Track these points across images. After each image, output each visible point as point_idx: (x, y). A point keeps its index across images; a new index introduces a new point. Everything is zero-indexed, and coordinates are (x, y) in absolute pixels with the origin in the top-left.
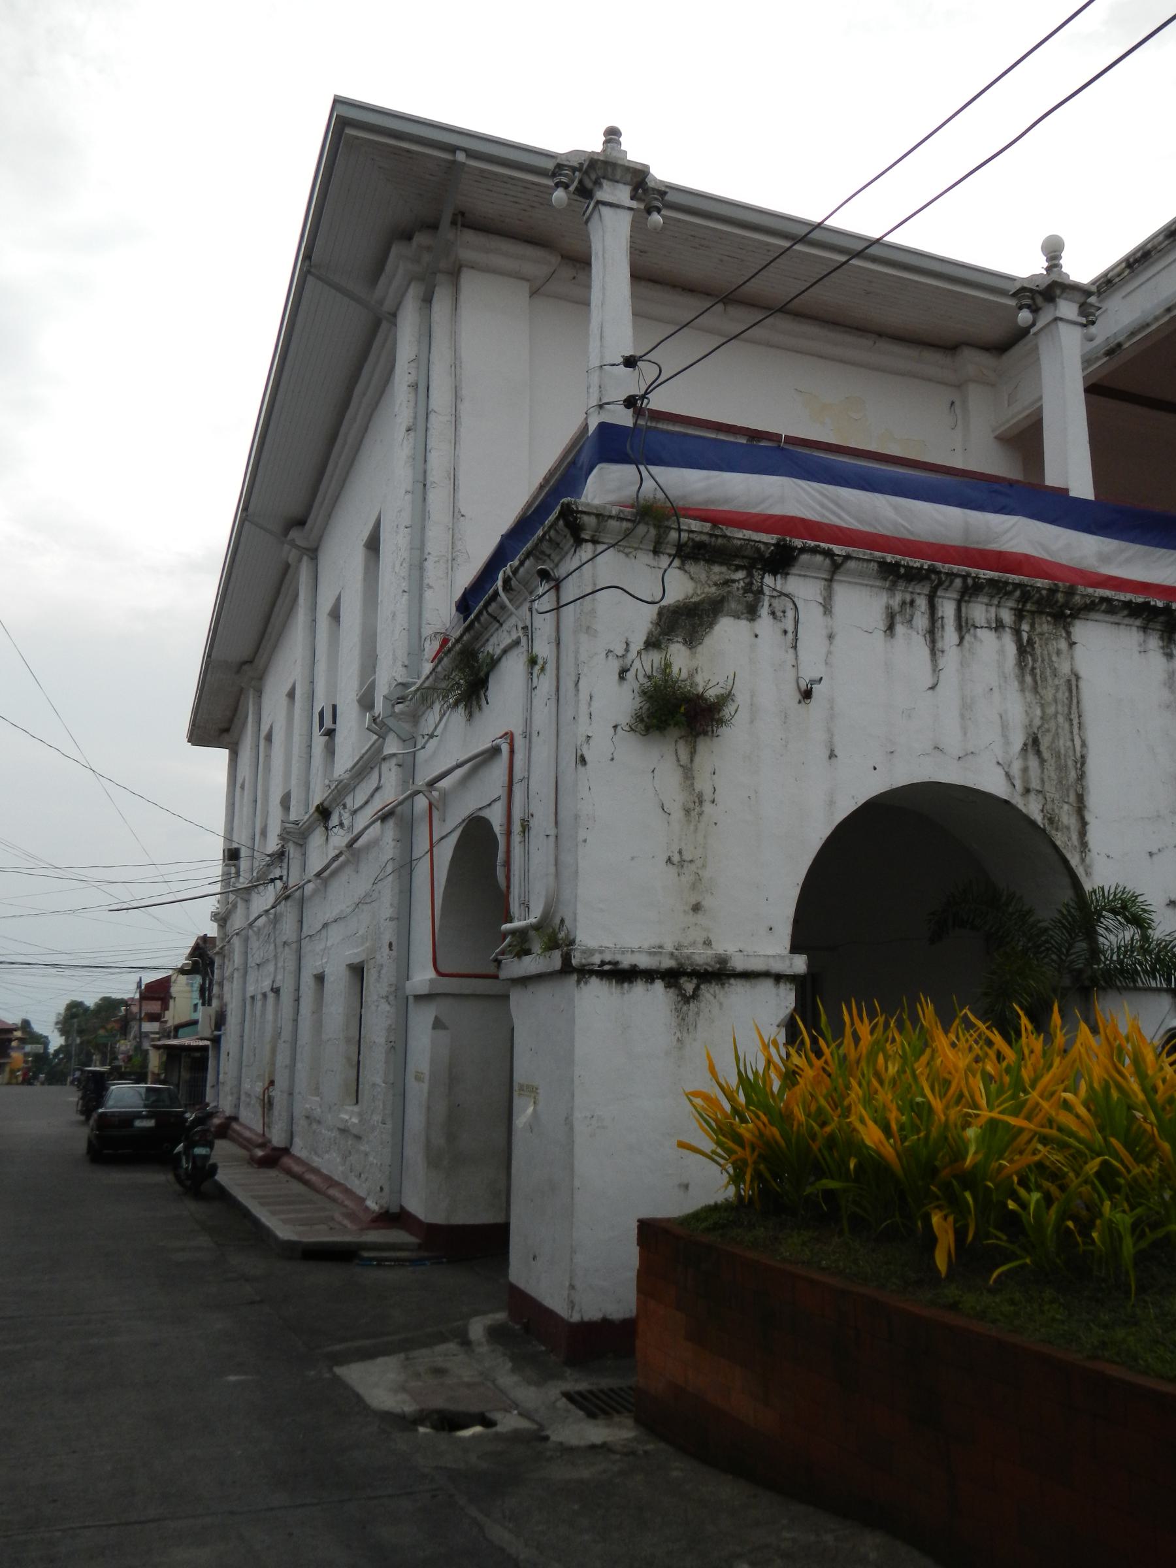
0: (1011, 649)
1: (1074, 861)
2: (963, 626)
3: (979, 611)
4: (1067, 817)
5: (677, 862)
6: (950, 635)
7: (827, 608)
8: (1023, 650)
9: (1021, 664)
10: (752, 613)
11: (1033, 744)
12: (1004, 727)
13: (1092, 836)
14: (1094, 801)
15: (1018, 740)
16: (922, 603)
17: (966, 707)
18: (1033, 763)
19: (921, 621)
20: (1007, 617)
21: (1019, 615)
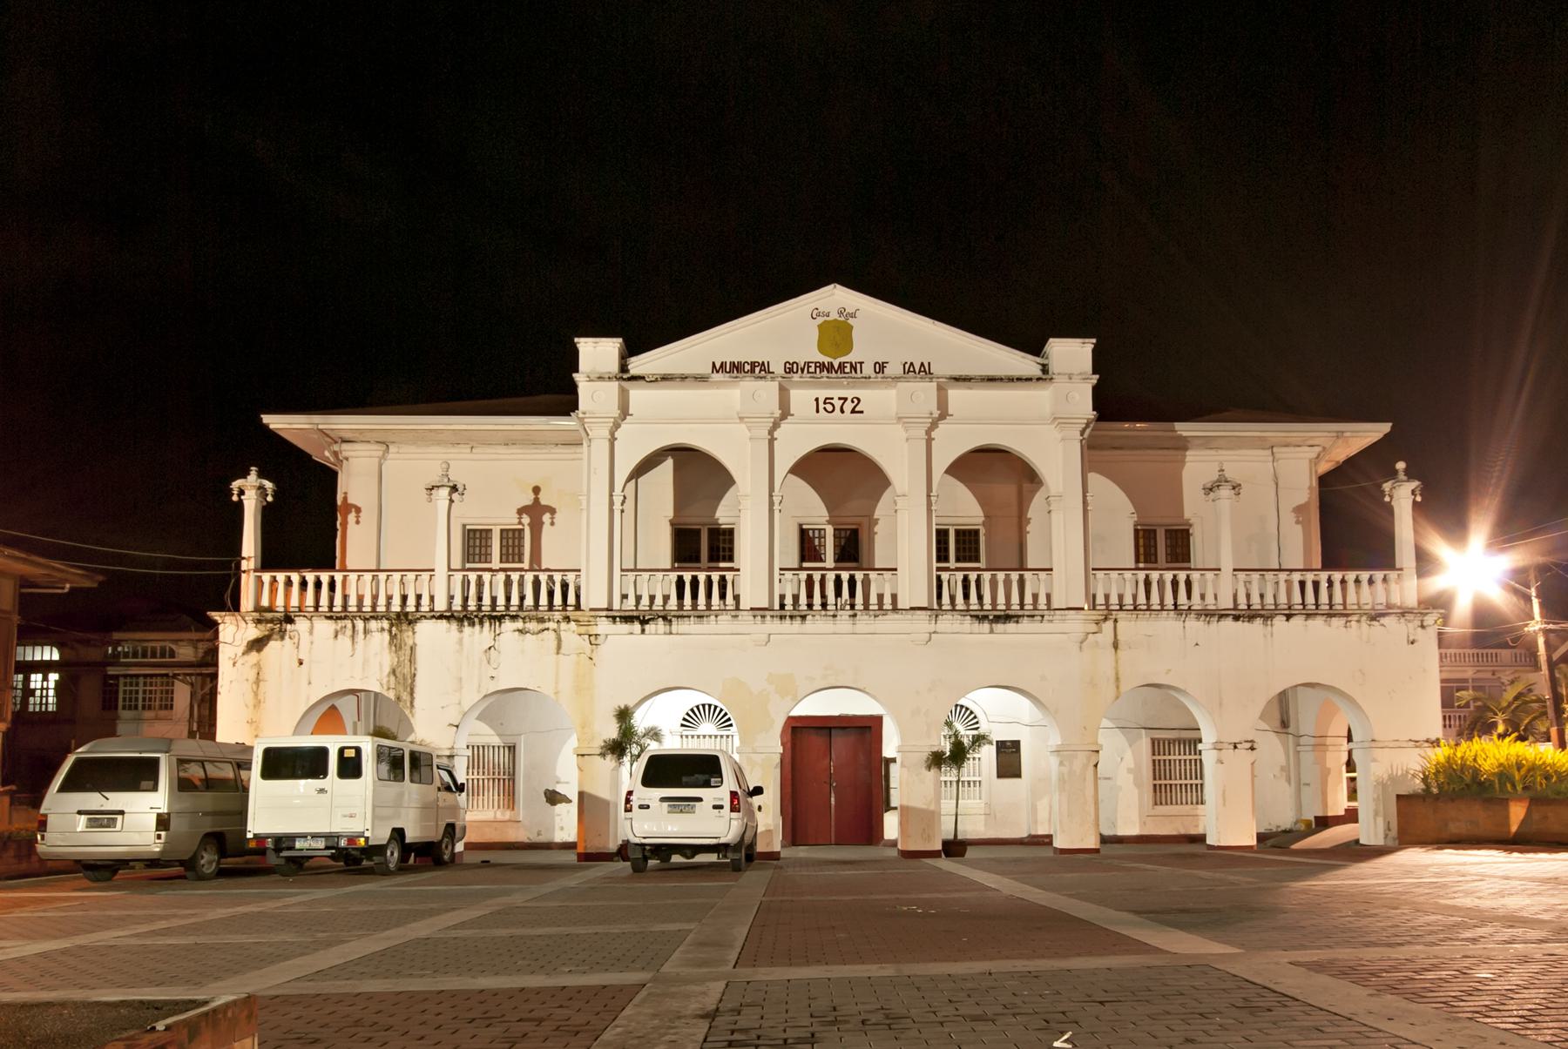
0: (386, 636)
1: (407, 712)
2: (366, 632)
3: (373, 624)
4: (405, 696)
5: (251, 722)
6: (361, 635)
7: (311, 632)
8: (393, 637)
9: (391, 643)
10: (282, 638)
11: (394, 672)
12: (381, 666)
13: (416, 703)
14: (417, 690)
15: (387, 670)
16: (349, 625)
17: (365, 662)
18: (392, 678)
19: (349, 632)
20: (386, 624)
21: (392, 625)
